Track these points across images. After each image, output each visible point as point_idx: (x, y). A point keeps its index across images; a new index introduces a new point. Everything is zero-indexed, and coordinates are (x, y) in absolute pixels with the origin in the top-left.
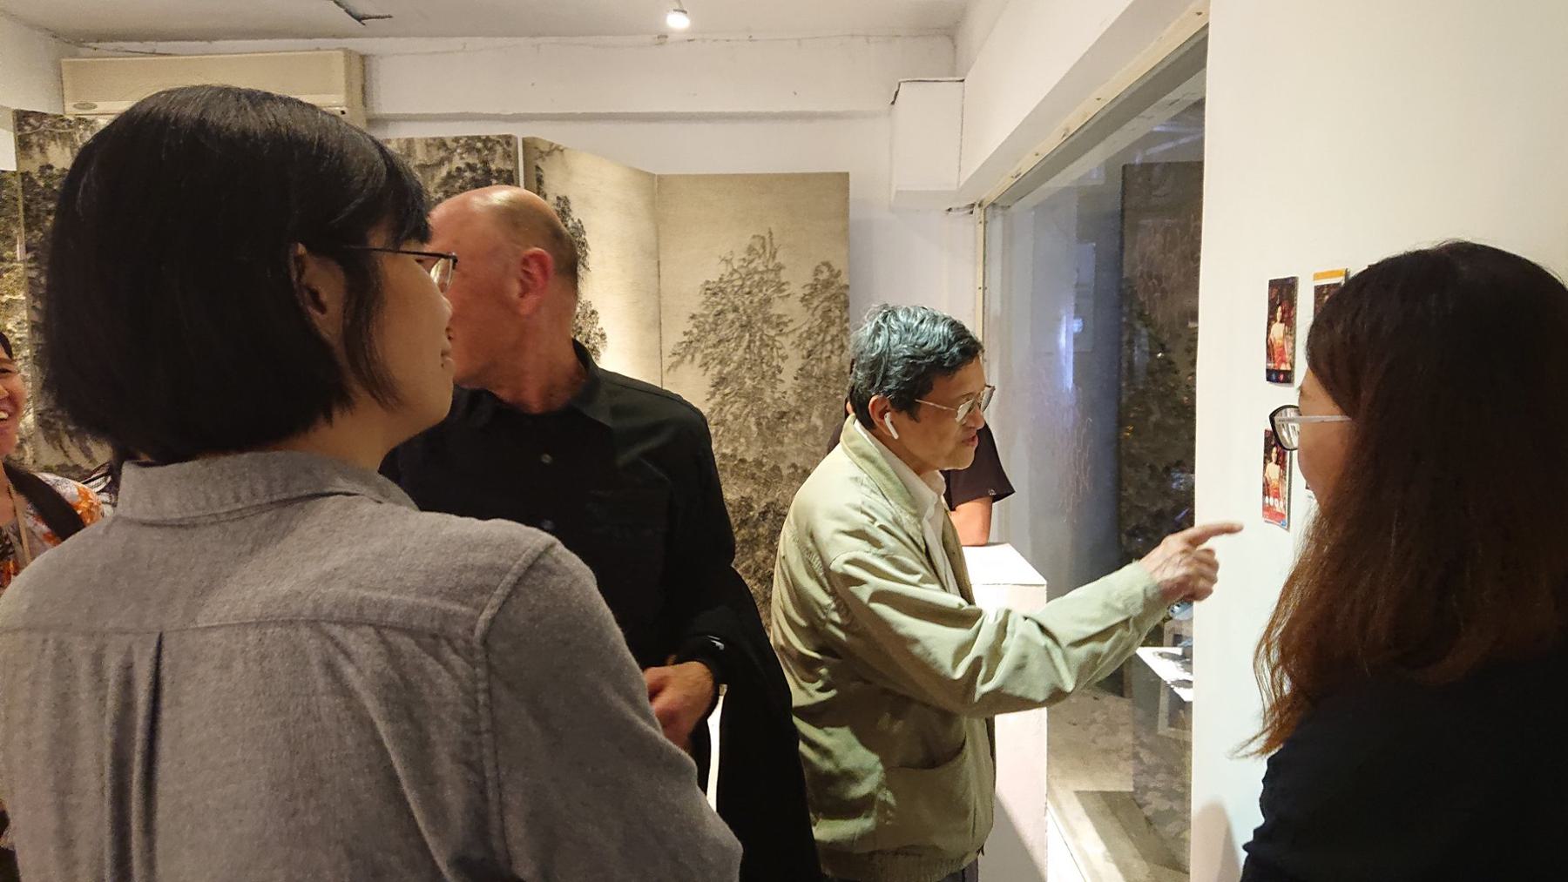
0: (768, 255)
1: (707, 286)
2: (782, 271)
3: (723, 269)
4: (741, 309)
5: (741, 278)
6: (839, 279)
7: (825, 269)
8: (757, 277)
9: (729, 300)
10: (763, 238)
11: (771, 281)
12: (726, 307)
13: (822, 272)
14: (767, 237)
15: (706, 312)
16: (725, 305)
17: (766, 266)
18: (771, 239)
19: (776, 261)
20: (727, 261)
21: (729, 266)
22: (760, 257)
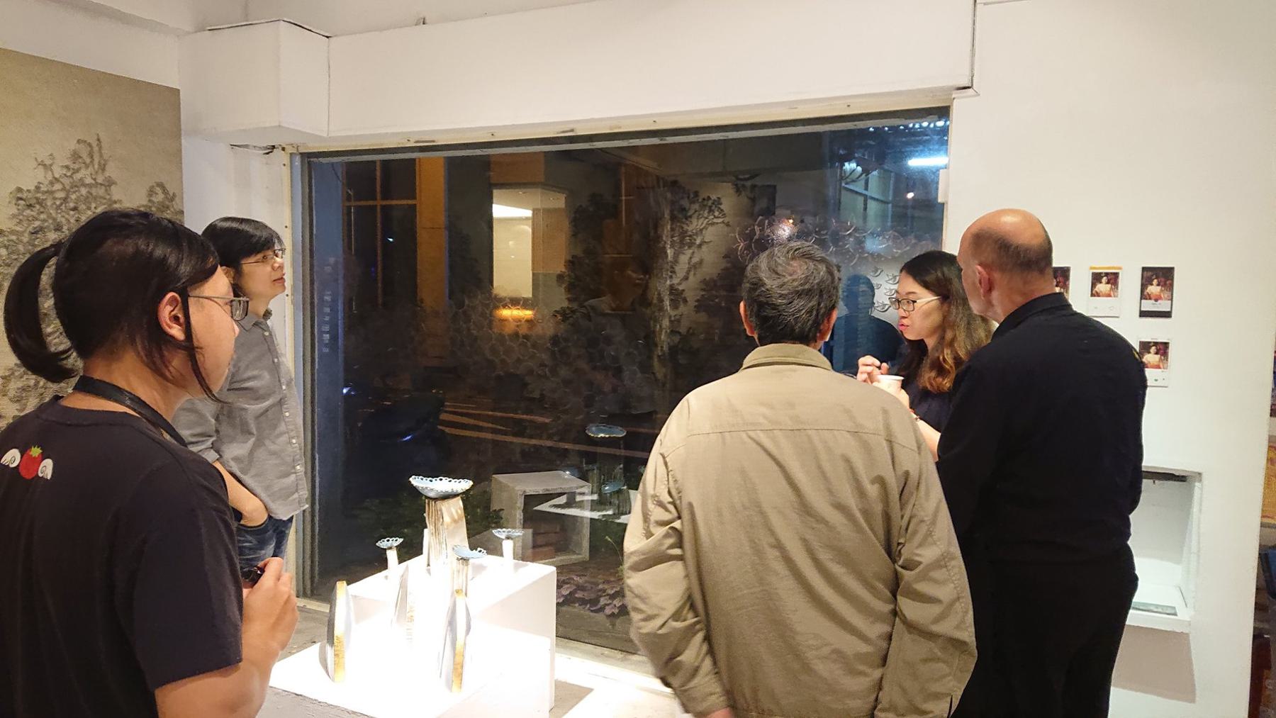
0: (96, 166)
1: (19, 195)
2: (113, 187)
3: (41, 176)
4: (65, 228)
5: (64, 189)
6: (174, 203)
7: (158, 190)
8: (84, 191)
9: (50, 216)
10: (90, 145)
11: (101, 197)
12: (46, 224)
13: (157, 194)
14: (94, 144)
15: (18, 228)
16: (44, 221)
17: (95, 179)
18: (100, 148)
19: (107, 174)
20: (45, 165)
21: (50, 173)
22: (87, 167)
